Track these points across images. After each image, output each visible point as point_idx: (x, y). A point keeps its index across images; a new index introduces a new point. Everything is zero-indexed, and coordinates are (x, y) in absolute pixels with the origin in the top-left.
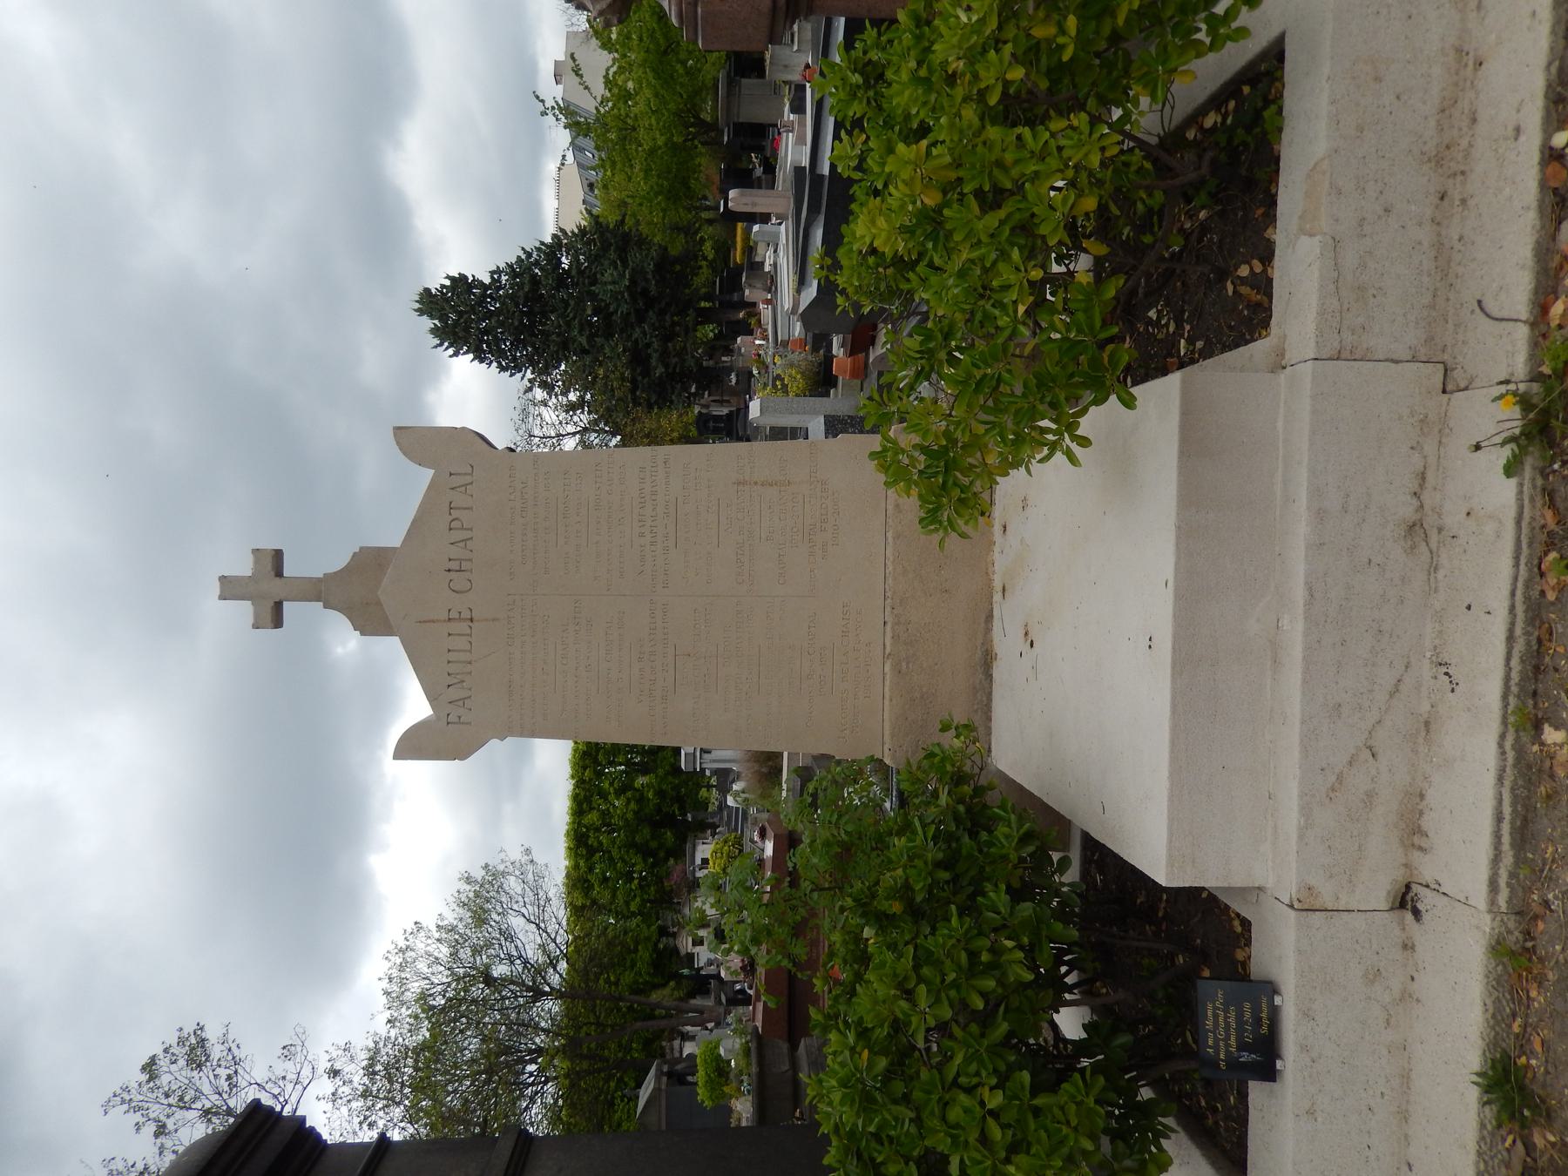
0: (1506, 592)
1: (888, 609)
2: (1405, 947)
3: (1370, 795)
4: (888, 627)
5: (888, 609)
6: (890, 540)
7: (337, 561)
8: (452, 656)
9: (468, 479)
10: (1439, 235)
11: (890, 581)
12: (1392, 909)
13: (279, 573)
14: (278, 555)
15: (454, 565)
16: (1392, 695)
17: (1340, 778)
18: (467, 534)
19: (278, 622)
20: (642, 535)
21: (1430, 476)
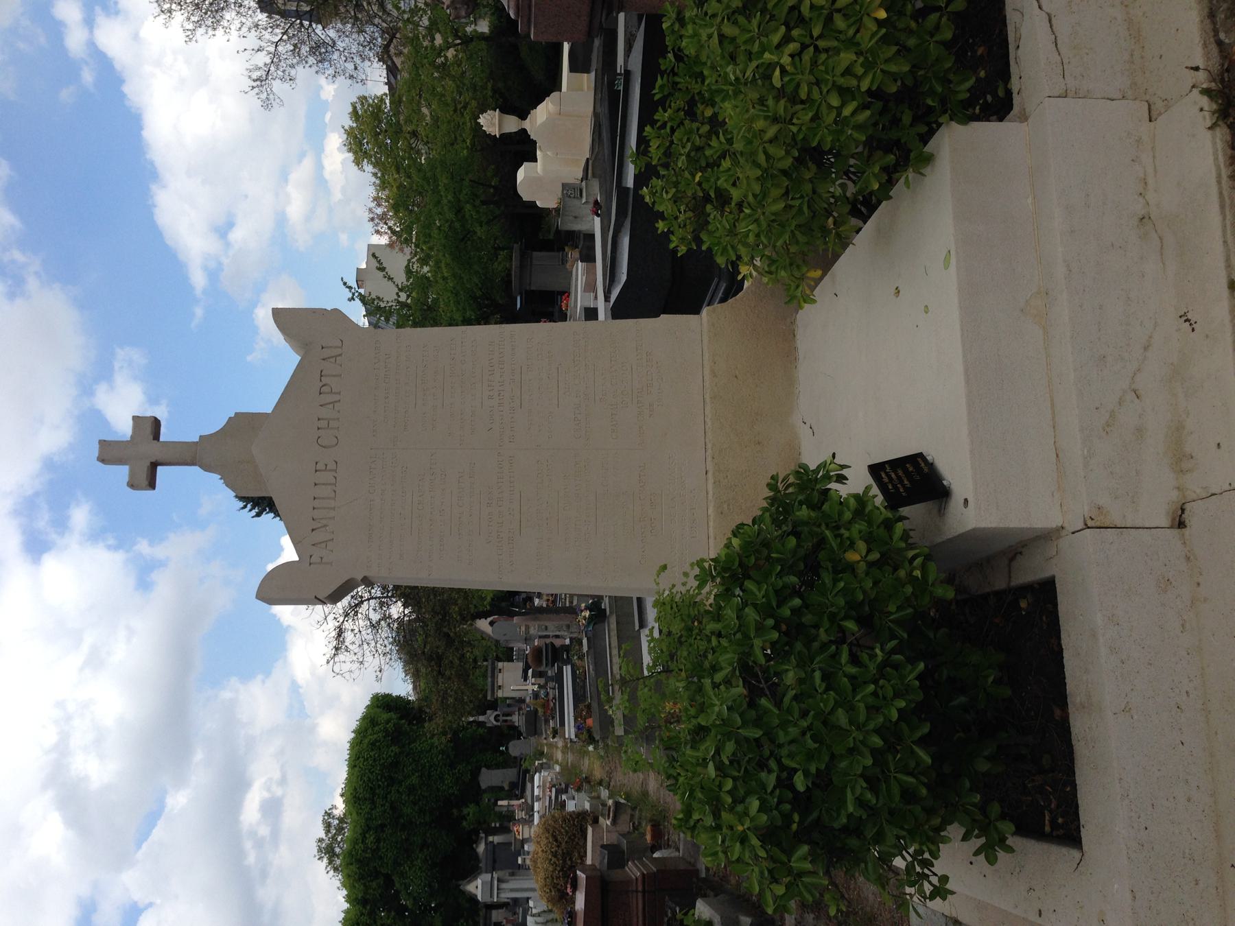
0: (1219, 233)
1: (709, 459)
2: (1188, 559)
3: (1140, 431)
4: (710, 474)
5: (709, 459)
6: (708, 400)
7: (214, 423)
8: (317, 503)
9: (339, 351)
10: (1128, 13)
11: (709, 434)
12: (1171, 527)
13: (156, 436)
14: (156, 423)
15: (323, 424)
16: (1146, 349)
17: (1112, 414)
18: (337, 397)
19: (152, 484)
20: (491, 397)
21: (1150, 181)
